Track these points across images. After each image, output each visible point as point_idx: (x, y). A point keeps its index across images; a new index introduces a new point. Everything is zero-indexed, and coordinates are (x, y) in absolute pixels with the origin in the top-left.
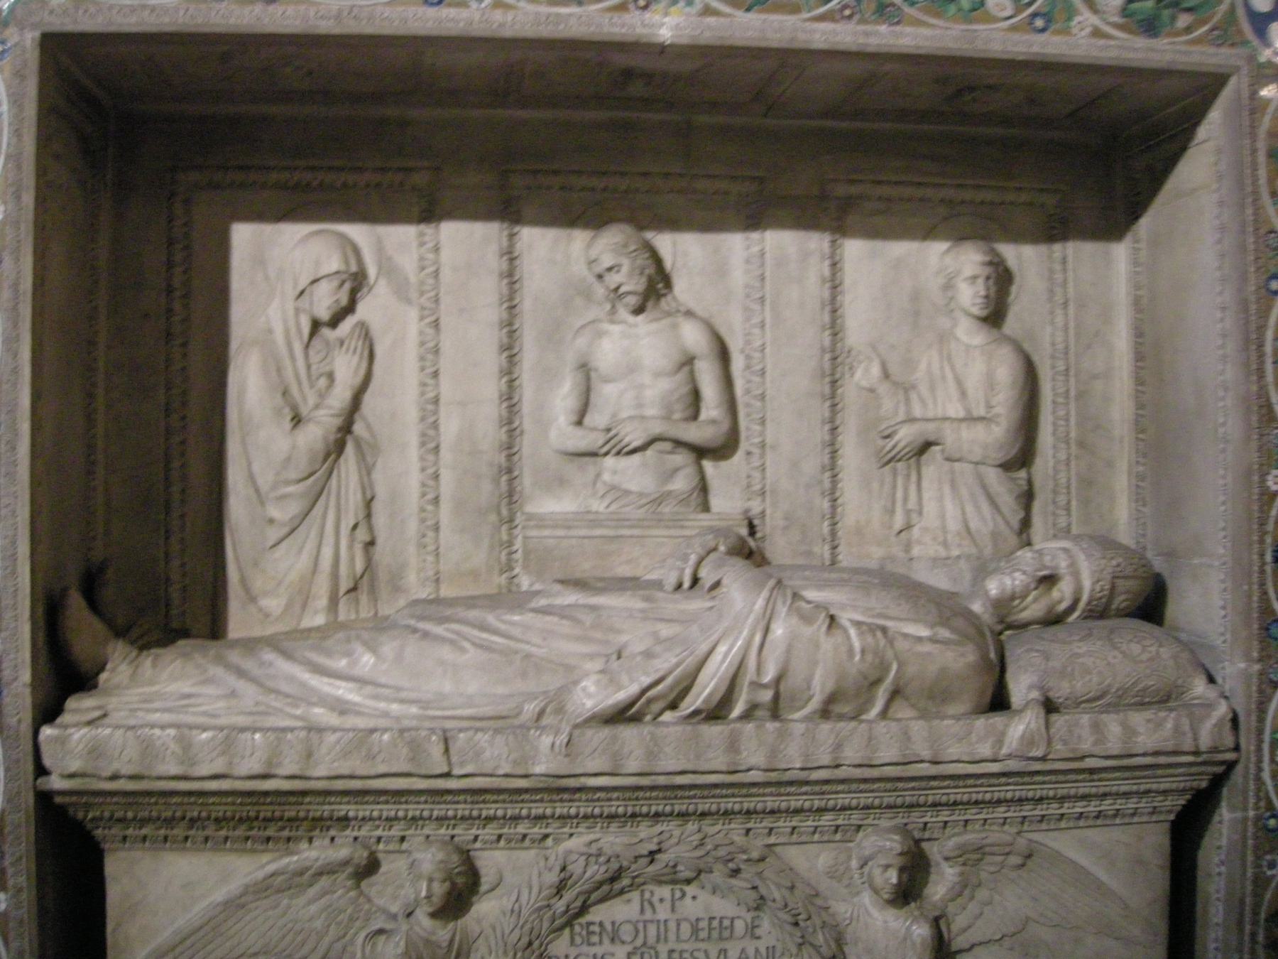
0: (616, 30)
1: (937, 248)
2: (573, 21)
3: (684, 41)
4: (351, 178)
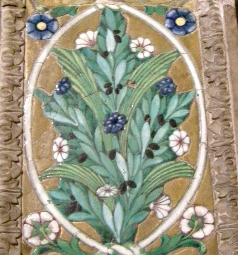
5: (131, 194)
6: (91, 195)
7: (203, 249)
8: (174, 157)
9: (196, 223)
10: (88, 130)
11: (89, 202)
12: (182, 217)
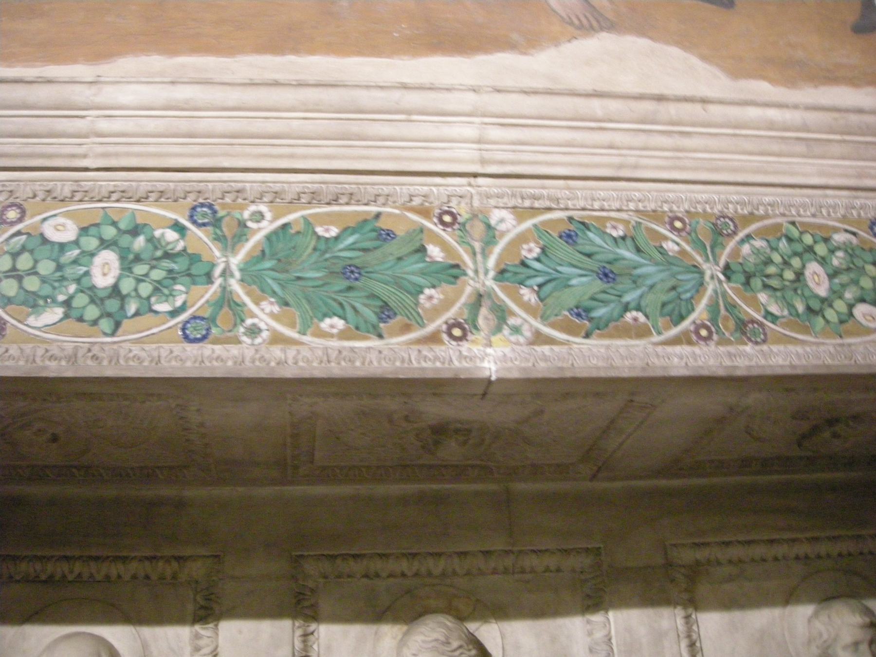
0: (428, 365)
1: (803, 612)
2: (373, 356)
3: (515, 375)
4: (115, 569)
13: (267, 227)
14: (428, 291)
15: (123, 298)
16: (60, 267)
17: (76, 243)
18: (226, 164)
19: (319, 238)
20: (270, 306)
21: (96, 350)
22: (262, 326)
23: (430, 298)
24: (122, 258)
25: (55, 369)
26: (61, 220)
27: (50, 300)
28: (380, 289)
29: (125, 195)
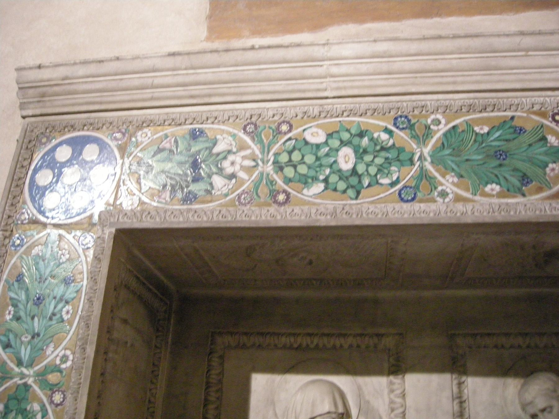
2: (521, 208)
5: (36, 340)
6: (18, 340)
7: (64, 374)
8: (63, 321)
9: (64, 359)
10: (25, 303)
11: (16, 343)
12: (58, 355)
13: (443, 128)
14: (551, 165)
15: (360, 176)
16: (318, 159)
17: (326, 143)
18: (413, 90)
19: (477, 134)
20: (451, 178)
21: (347, 208)
22: (448, 190)
23: (553, 170)
24: (356, 152)
25: (324, 221)
26: (314, 130)
27: (315, 179)
28: (520, 165)
29: (352, 113)
